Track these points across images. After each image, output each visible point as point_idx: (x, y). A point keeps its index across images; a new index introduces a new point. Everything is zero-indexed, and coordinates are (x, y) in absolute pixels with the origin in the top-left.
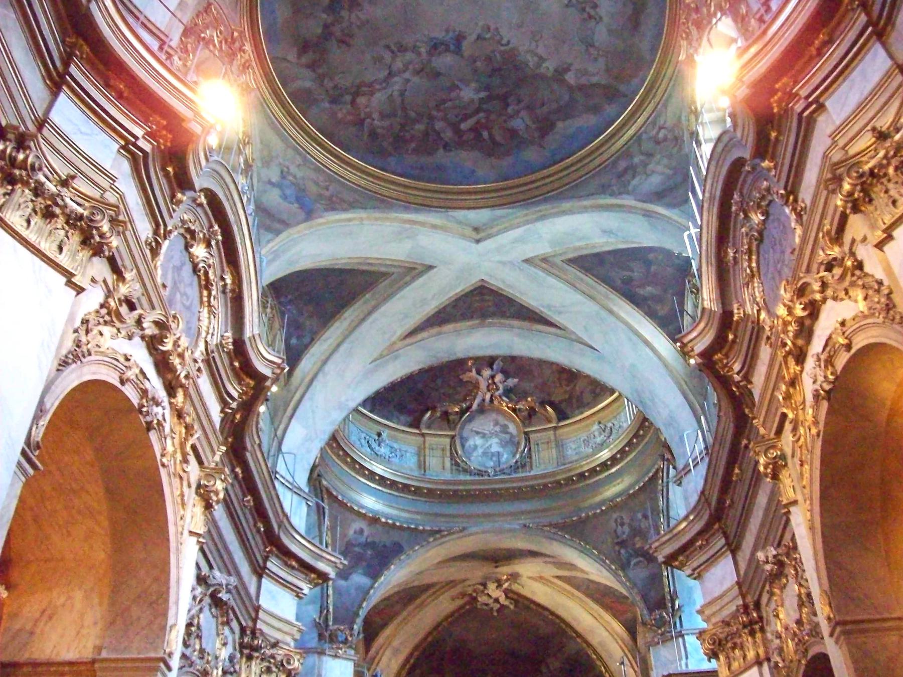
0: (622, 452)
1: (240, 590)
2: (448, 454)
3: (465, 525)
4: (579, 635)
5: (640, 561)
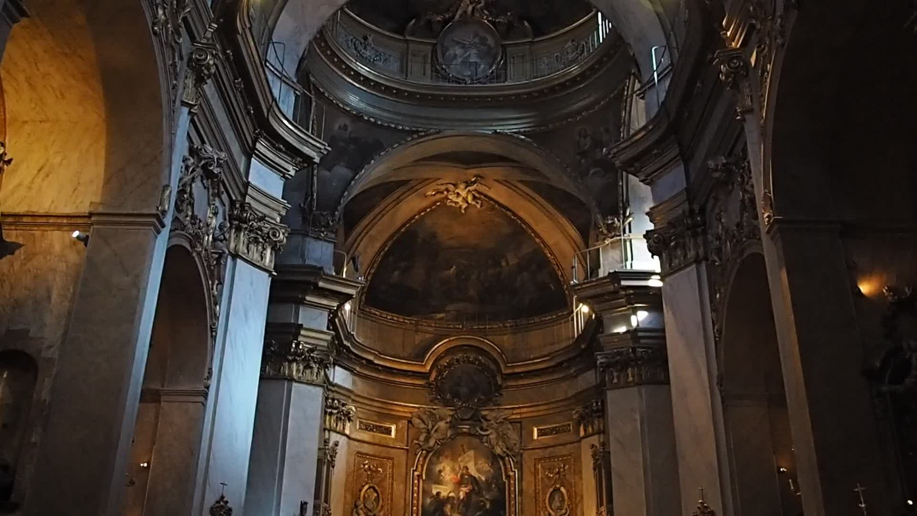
0: (591, 68)
1: (230, 165)
2: (429, 61)
3: (442, 128)
4: (538, 236)
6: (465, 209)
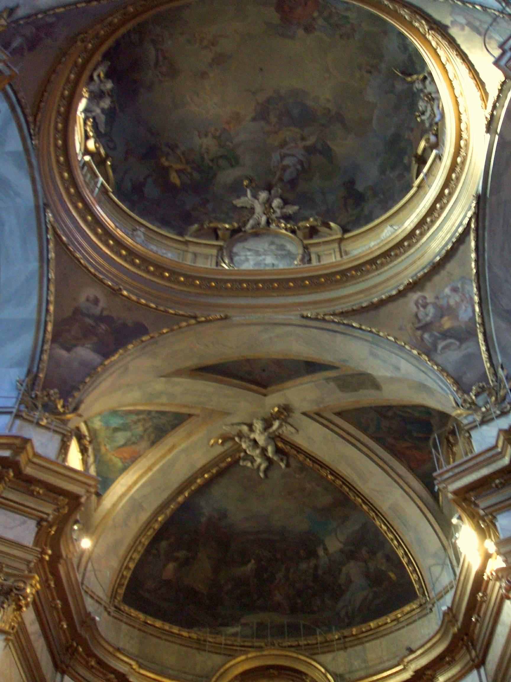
4: (366, 501)
5: (451, 344)
6: (266, 471)
